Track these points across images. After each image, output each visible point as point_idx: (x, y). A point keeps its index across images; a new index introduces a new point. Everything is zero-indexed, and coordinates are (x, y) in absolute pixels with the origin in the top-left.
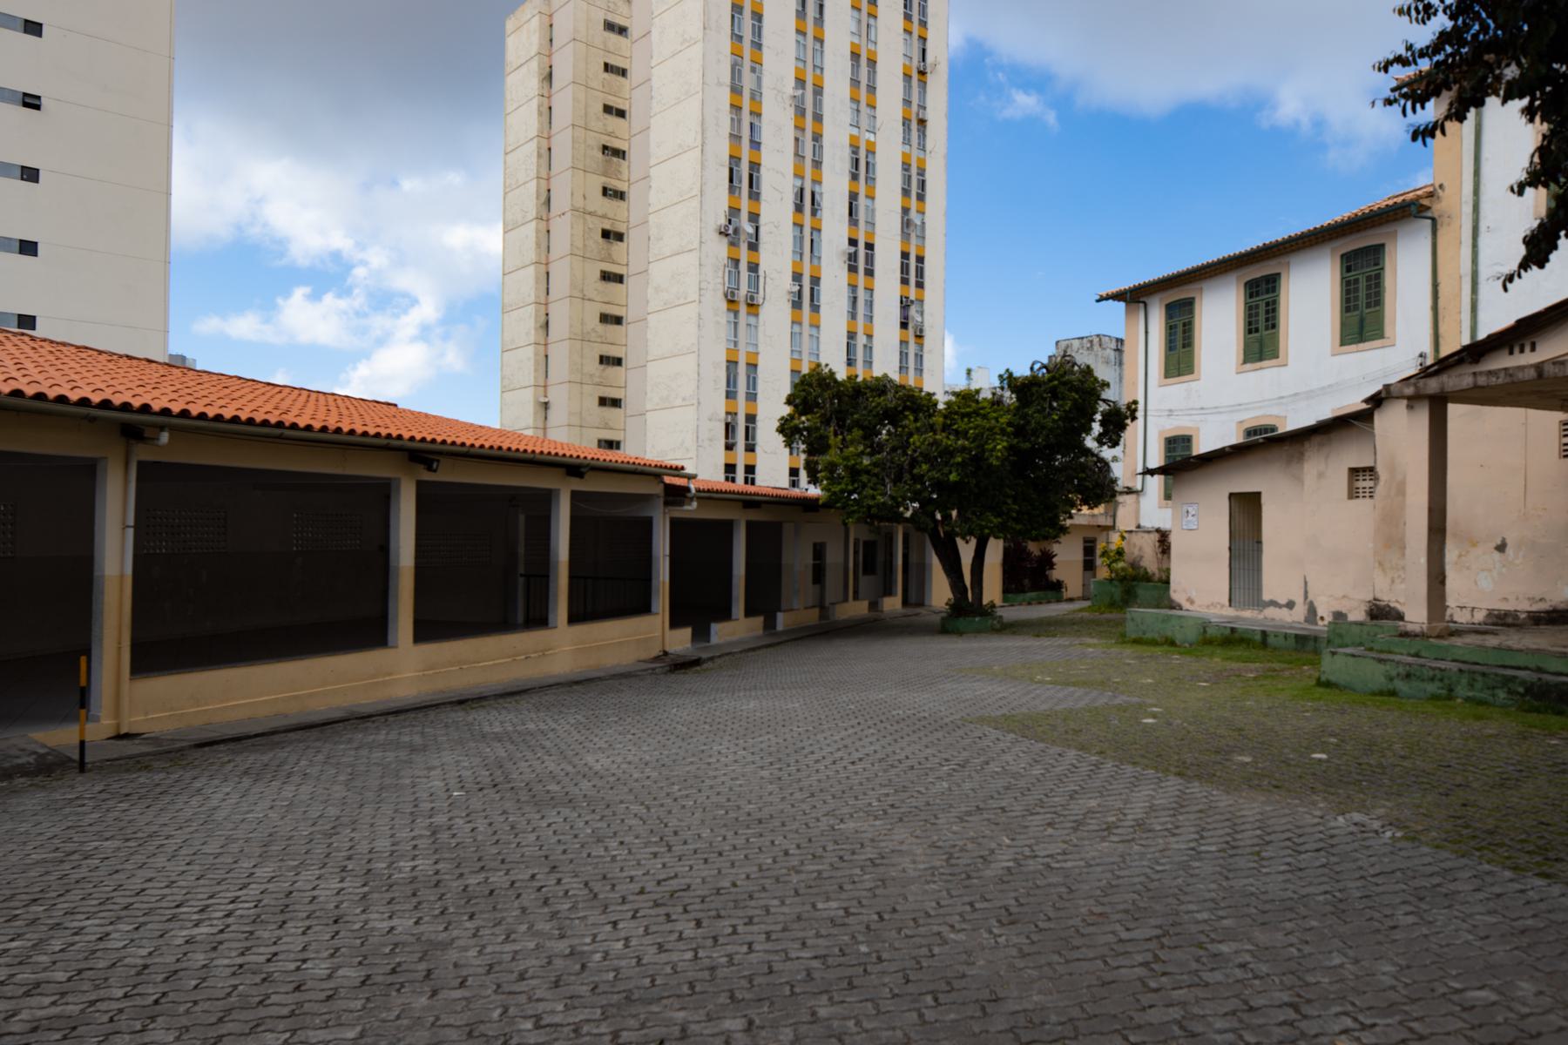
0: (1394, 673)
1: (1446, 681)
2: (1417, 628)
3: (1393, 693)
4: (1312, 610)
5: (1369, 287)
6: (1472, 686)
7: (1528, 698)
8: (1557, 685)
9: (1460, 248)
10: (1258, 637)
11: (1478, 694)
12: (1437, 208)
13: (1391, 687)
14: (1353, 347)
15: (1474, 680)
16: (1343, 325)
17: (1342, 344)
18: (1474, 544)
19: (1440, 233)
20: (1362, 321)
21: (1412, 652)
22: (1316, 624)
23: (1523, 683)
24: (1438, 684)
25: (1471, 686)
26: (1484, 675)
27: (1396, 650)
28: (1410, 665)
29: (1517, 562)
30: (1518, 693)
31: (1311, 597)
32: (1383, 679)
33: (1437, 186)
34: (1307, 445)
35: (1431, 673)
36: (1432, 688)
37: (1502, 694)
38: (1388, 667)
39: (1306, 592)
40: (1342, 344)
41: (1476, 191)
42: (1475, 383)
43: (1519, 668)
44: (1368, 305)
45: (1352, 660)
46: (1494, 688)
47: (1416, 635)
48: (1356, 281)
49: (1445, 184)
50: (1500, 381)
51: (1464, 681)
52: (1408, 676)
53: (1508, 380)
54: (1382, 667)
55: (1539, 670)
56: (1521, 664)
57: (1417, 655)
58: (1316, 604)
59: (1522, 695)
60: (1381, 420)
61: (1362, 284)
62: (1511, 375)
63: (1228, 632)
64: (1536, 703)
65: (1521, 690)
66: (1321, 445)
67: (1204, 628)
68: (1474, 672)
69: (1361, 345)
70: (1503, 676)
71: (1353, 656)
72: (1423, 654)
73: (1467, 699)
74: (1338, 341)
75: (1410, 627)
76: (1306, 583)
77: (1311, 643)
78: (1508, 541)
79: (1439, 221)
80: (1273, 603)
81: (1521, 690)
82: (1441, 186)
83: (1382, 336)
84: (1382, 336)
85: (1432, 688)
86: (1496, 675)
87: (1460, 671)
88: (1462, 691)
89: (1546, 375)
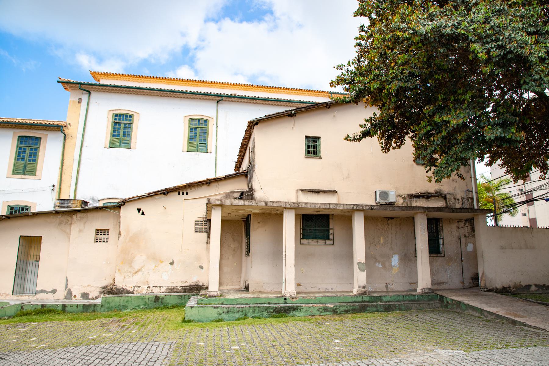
0: (221, 312)
1: (244, 312)
2: (215, 294)
3: (221, 320)
4: (70, 293)
5: (31, 153)
6: (254, 312)
7: (274, 313)
8: (284, 307)
9: (75, 149)
10: (60, 308)
11: (256, 315)
12: (66, 132)
13: (220, 318)
14: (19, 176)
15: (255, 309)
16: (15, 165)
17: (13, 174)
18: (161, 262)
19: (67, 141)
20: (25, 166)
21: (220, 303)
22: (72, 299)
23: (273, 308)
24: (240, 313)
25: (254, 312)
26: (259, 307)
27: (213, 303)
28: (229, 307)
29: (178, 269)
30: (271, 312)
31: (69, 287)
32: (216, 315)
33: (68, 124)
34: (74, 217)
35: (238, 309)
36: (238, 315)
37: (265, 313)
38: (219, 310)
39: (67, 285)
40: (13, 174)
41: (84, 131)
42: (244, 204)
43: (262, 304)
44: (30, 160)
45: (201, 309)
46: (262, 312)
47: (215, 296)
48: (25, 149)
49: (71, 124)
50: (253, 204)
51: (251, 311)
52: (228, 312)
53: (256, 205)
54: (216, 310)
55: (269, 303)
56: (263, 302)
57: (222, 304)
58: (72, 290)
59: (273, 313)
60: (123, 210)
61: (28, 151)
62: (257, 203)
63: (40, 307)
64: (277, 315)
65: (272, 311)
66: (81, 218)
67: (22, 307)
68: (255, 307)
69: (23, 176)
70: (266, 306)
71: (202, 307)
72: (225, 303)
73: (253, 317)
74: (11, 172)
75: (212, 294)
76: (67, 280)
77: (93, 308)
78: (174, 261)
79: (67, 137)
80: (43, 291)
81: (272, 311)
82: (69, 124)
83: (35, 175)
84: (35, 175)
85: (238, 315)
86: (263, 307)
87: (250, 307)
88: (250, 314)
89: (268, 205)
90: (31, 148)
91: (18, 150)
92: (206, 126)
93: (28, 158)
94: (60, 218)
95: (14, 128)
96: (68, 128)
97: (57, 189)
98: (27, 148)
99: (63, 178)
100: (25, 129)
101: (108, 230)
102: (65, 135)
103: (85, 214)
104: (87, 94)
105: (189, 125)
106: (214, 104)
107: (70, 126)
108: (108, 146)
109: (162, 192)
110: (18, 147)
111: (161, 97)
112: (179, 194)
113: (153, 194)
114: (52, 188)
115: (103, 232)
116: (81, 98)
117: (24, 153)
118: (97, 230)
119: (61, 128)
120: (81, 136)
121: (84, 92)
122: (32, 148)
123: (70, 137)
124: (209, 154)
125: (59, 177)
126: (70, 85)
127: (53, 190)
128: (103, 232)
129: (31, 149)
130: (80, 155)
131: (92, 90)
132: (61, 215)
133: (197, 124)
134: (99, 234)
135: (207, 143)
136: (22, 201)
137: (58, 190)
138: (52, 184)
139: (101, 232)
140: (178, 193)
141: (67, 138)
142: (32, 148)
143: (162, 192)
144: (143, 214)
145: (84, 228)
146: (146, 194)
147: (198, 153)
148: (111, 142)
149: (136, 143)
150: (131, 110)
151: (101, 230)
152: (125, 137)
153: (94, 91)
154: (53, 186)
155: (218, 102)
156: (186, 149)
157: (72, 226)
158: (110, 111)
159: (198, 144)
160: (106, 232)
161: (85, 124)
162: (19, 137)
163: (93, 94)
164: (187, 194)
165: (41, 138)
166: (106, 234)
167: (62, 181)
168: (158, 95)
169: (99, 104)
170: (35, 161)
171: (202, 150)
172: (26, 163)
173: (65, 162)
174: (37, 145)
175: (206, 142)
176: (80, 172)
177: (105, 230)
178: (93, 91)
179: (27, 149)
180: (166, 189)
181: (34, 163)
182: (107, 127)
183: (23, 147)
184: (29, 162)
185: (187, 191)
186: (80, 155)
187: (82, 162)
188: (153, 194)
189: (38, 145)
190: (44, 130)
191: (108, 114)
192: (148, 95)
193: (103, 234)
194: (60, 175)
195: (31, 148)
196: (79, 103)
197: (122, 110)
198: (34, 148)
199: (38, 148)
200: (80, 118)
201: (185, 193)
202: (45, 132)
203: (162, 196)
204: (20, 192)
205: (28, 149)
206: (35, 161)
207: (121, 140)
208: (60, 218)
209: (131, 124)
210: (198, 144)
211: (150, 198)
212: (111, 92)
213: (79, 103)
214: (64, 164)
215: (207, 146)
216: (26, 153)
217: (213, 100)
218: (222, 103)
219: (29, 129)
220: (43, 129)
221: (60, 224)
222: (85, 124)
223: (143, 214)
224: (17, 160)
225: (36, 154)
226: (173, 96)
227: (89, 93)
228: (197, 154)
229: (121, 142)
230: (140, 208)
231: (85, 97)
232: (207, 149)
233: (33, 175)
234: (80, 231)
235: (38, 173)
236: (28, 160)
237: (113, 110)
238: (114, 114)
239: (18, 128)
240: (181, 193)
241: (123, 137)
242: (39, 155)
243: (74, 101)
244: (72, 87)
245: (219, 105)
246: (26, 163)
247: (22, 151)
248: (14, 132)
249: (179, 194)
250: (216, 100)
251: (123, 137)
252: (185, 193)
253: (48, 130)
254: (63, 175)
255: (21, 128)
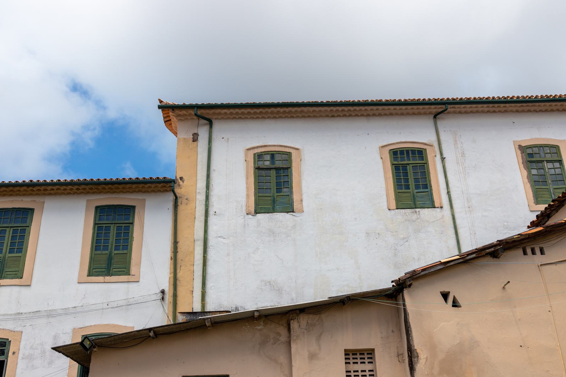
5: (118, 234)
12: (177, 190)
14: (101, 279)
16: (92, 260)
17: (89, 275)
19: (181, 208)
20: (110, 259)
33: (178, 178)
40: (89, 275)
44: (117, 248)
48: (108, 229)
61: (113, 231)
69: (108, 278)
74: (86, 272)
79: (179, 200)
82: (181, 178)
83: (128, 273)
84: (128, 273)
90: (118, 225)
91: (96, 232)
92: (423, 160)
93: (114, 245)
94: (260, 330)
95: (88, 193)
96: (179, 185)
97: (169, 297)
98: (112, 226)
99: (180, 274)
100: (107, 192)
101: (371, 352)
102: (176, 197)
103: (316, 317)
104: (205, 124)
105: (391, 162)
106: (429, 122)
107: (183, 182)
108: (252, 210)
109: (493, 249)
110: (97, 226)
111: (333, 118)
112: (525, 253)
113: (474, 255)
114: (160, 296)
115: (358, 356)
116: (196, 132)
117: (107, 234)
118: (347, 353)
119: (172, 184)
120: (204, 197)
121: (203, 121)
122: (121, 225)
123: (184, 201)
124: (438, 210)
125: (172, 275)
126: (178, 112)
127: (163, 299)
128: (358, 356)
129: (119, 228)
130: (206, 231)
131: (215, 117)
132: (262, 323)
133: (406, 158)
134: (351, 361)
135: (431, 190)
136: (108, 325)
137: (171, 299)
138: (161, 289)
139: (355, 356)
140: (521, 251)
141: (179, 204)
142: (121, 225)
143: (493, 249)
144: (455, 304)
145: (320, 348)
146: (458, 257)
147: (417, 210)
148: (257, 204)
149: (302, 201)
150: (285, 145)
151: (354, 352)
152: (280, 192)
153: (218, 119)
154: (163, 292)
155: (435, 117)
156: (393, 204)
157: (293, 346)
158: (248, 150)
159: (413, 194)
160: (366, 356)
161: (208, 176)
162: (97, 208)
163: (217, 126)
164: (542, 252)
165: (133, 207)
166: (367, 361)
167: (178, 283)
168: (327, 116)
169: (228, 139)
170: (127, 249)
171: (423, 203)
172: (111, 253)
173: (179, 245)
174: (128, 219)
175: (427, 188)
176: (210, 263)
177: (362, 352)
178: (216, 119)
179: (112, 228)
180: (500, 242)
181: (125, 251)
182: (247, 178)
183: (104, 225)
184: (116, 252)
185: (541, 246)
186: (206, 231)
187: (212, 241)
188: (474, 255)
189: (131, 219)
190: (140, 191)
191: (246, 155)
192: (309, 117)
193: (359, 361)
194: (172, 270)
195: (118, 225)
196: (194, 141)
197: (270, 146)
198: (123, 225)
199: (131, 225)
200: (199, 167)
201: (538, 251)
202: (140, 196)
203: (489, 260)
204: (103, 309)
205: (114, 227)
206: (127, 249)
207: (274, 199)
208: (260, 330)
209: (287, 168)
210: (413, 194)
211: (464, 267)
212: (246, 118)
213: (194, 141)
214: (179, 250)
215: (432, 194)
216: (111, 235)
217: (425, 114)
218: (443, 119)
219: (114, 192)
220: (137, 190)
221: (263, 343)
222: (208, 176)
223: (455, 304)
224: (96, 250)
225: (128, 236)
226: (354, 114)
227: (210, 123)
228: (416, 212)
229: (274, 201)
230: (446, 290)
231: (203, 133)
232: (433, 202)
233: (125, 275)
234: (312, 357)
235: (133, 270)
236: (114, 247)
237: (254, 148)
238: (256, 155)
239: (94, 193)
240: (529, 251)
241: (277, 192)
242: (132, 237)
243: (185, 139)
244: (180, 115)
245: (439, 123)
246: (111, 253)
247: (104, 232)
248: (88, 201)
249: (525, 253)
250: (430, 113)
251: (277, 192)
252: (538, 251)
253: (145, 192)
254: (178, 271)
255: (100, 193)
